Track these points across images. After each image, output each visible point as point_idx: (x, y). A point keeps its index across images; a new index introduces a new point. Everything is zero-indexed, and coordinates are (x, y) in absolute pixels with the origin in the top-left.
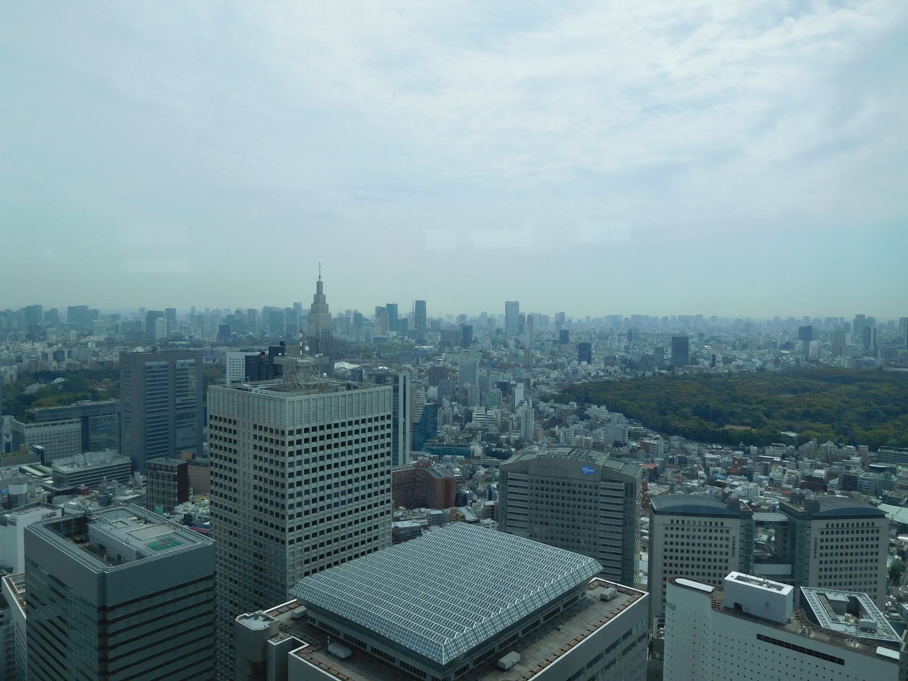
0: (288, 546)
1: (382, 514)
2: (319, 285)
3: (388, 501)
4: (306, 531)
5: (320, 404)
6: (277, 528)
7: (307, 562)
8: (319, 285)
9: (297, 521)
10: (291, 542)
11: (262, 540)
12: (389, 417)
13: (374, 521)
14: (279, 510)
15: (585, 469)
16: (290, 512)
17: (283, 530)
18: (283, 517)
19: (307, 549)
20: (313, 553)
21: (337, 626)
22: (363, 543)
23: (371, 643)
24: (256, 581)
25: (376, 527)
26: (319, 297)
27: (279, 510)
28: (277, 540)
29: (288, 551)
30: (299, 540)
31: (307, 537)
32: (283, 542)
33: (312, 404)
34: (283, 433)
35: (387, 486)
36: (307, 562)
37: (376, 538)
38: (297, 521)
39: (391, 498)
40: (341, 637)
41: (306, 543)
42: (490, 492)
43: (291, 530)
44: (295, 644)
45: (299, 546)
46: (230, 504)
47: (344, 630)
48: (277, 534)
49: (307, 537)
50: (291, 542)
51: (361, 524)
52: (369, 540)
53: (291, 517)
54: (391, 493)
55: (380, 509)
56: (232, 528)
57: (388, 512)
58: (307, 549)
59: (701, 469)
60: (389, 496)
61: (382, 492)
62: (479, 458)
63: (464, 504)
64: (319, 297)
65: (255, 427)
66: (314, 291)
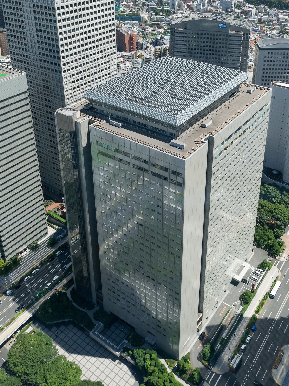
0: (63, 74)
1: (111, 54)
3: (114, 47)
6: (55, 64)
7: (74, 82)
9: (66, 60)
10: (65, 71)
11: (47, 72)
13: (107, 59)
16: (62, 55)
18: (59, 58)
19: (73, 75)
20: (76, 77)
22: (102, 70)
24: (45, 94)
25: (109, 61)
28: (56, 71)
29: (63, 77)
34: (53, 9)
36: (74, 82)
37: (109, 68)
38: (66, 60)
39: (116, 45)
41: (72, 72)
46: (24, 53)
48: (56, 68)
50: (65, 71)
51: (101, 60)
52: (106, 69)
54: (115, 42)
56: (27, 66)
57: (115, 53)
58: (73, 75)
60: (115, 44)
61: (111, 42)
63: (142, 48)
65: (34, 5)
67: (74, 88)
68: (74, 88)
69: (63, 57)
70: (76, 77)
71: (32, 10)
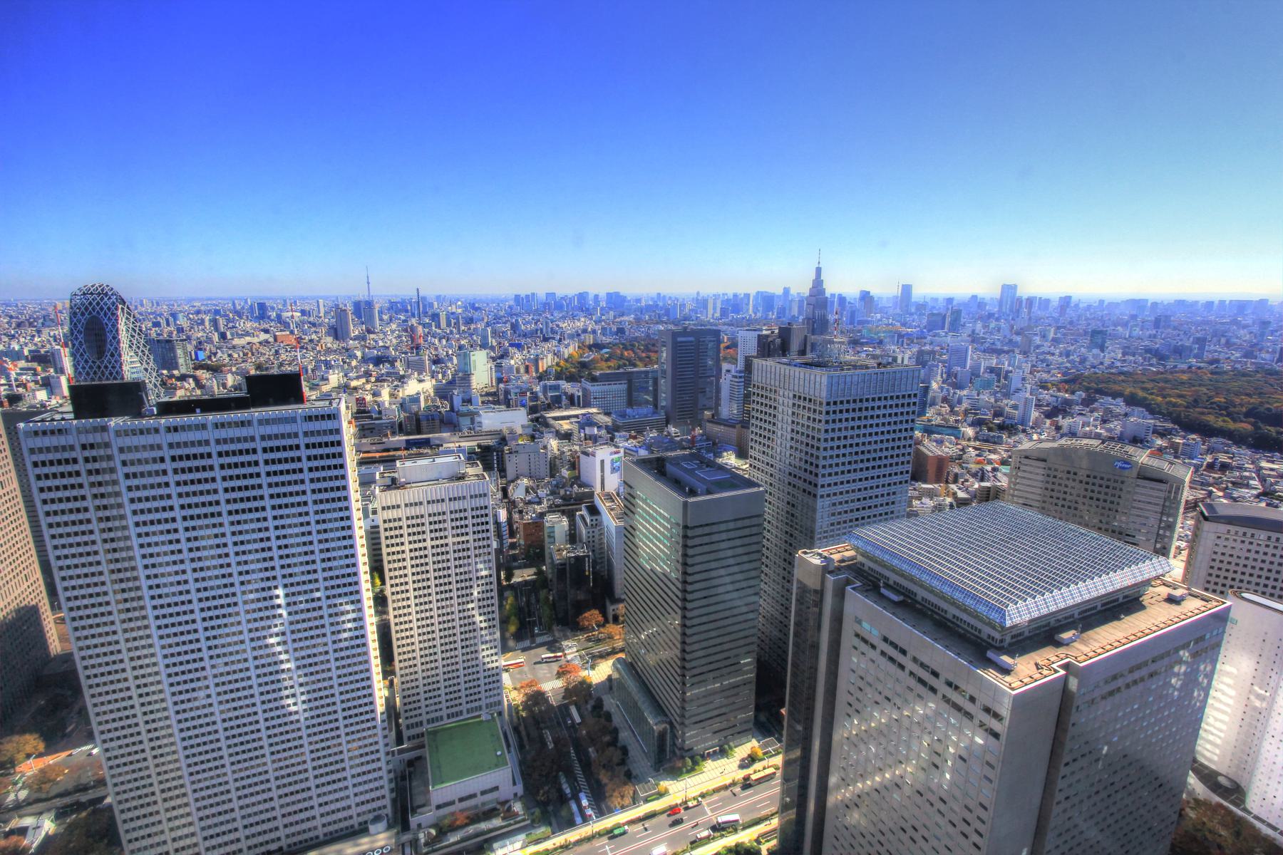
0: (819, 500)
2: (819, 271)
4: (834, 489)
5: (855, 378)
8: (819, 271)
9: (828, 480)
10: (822, 496)
11: (795, 492)
12: (915, 395)
13: (893, 488)
14: (813, 469)
15: (1120, 464)
16: (823, 471)
17: (816, 485)
20: (839, 508)
21: (887, 573)
23: (921, 593)
26: (818, 283)
27: (813, 469)
30: (828, 495)
31: (835, 494)
32: (815, 496)
33: (848, 379)
35: (907, 458)
36: (833, 514)
38: (828, 480)
40: (891, 582)
42: (983, 473)
43: (823, 486)
44: (848, 582)
45: (827, 501)
47: (893, 578)
49: (835, 494)
50: (822, 496)
53: (823, 476)
55: (899, 478)
58: (834, 504)
59: (1253, 479)
60: (909, 467)
62: (969, 440)
64: (818, 283)
66: (814, 277)
67: (832, 524)
68: (832, 524)
69: (823, 476)
70: (839, 508)
71: (791, 403)
